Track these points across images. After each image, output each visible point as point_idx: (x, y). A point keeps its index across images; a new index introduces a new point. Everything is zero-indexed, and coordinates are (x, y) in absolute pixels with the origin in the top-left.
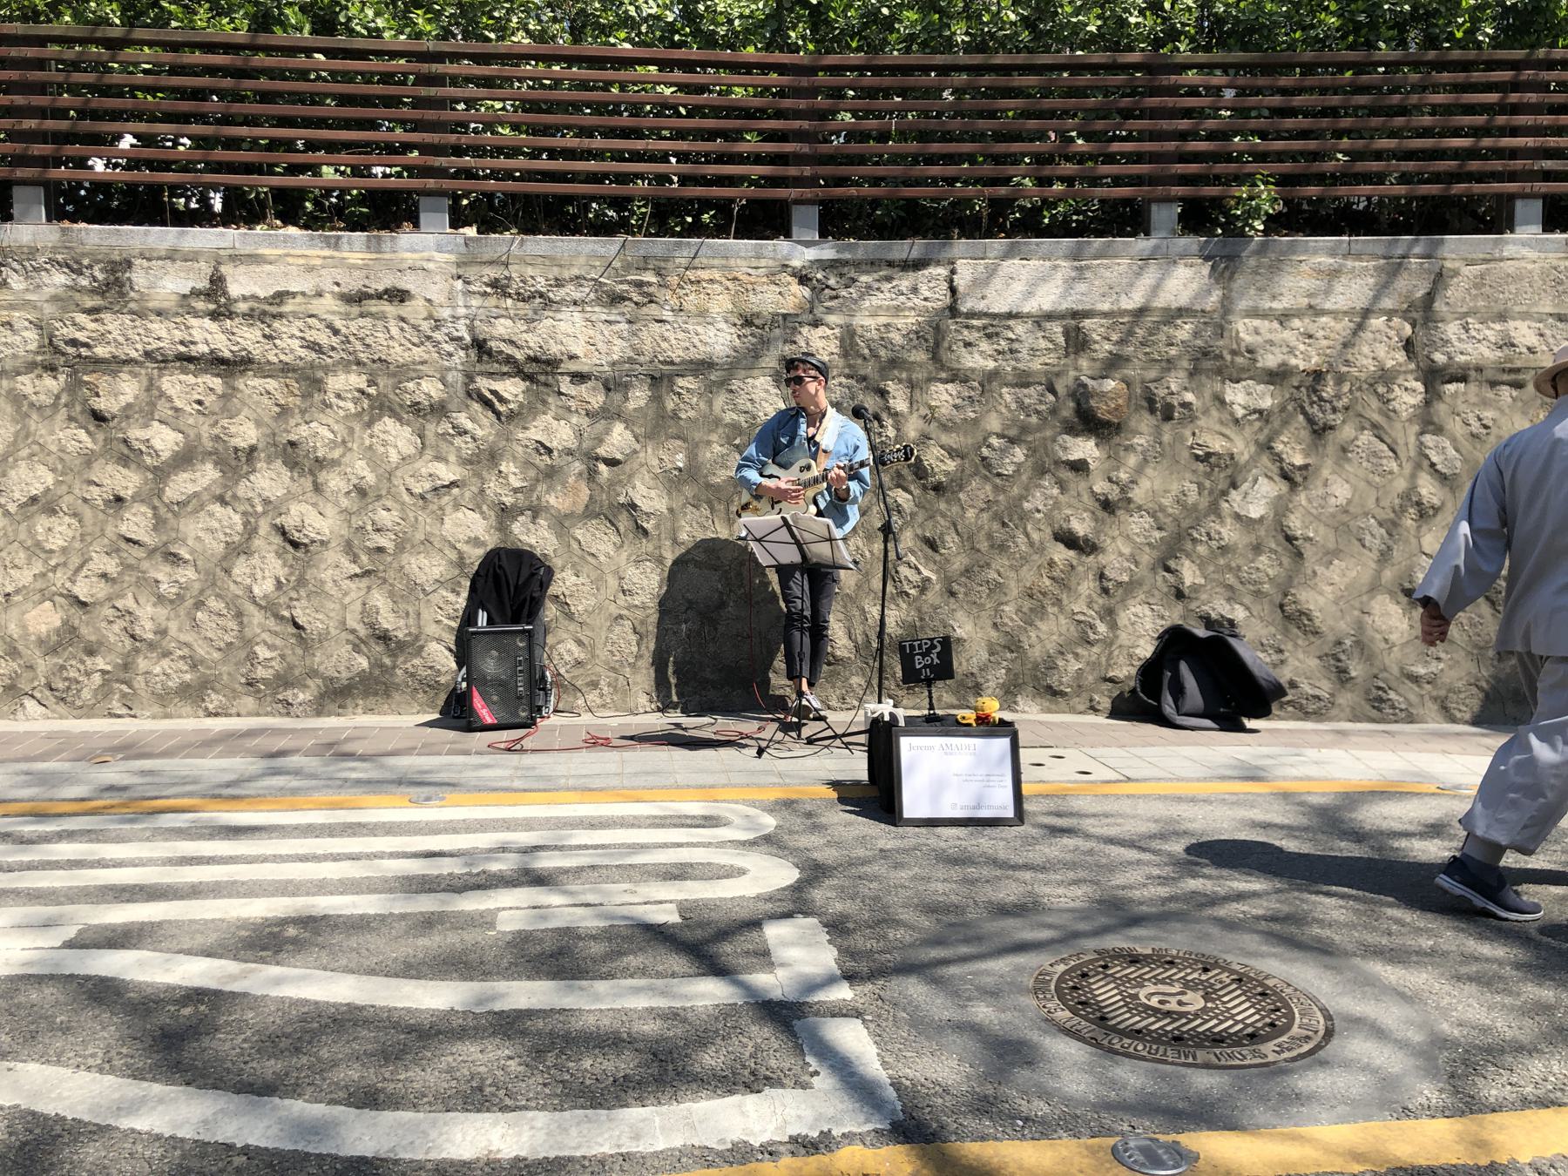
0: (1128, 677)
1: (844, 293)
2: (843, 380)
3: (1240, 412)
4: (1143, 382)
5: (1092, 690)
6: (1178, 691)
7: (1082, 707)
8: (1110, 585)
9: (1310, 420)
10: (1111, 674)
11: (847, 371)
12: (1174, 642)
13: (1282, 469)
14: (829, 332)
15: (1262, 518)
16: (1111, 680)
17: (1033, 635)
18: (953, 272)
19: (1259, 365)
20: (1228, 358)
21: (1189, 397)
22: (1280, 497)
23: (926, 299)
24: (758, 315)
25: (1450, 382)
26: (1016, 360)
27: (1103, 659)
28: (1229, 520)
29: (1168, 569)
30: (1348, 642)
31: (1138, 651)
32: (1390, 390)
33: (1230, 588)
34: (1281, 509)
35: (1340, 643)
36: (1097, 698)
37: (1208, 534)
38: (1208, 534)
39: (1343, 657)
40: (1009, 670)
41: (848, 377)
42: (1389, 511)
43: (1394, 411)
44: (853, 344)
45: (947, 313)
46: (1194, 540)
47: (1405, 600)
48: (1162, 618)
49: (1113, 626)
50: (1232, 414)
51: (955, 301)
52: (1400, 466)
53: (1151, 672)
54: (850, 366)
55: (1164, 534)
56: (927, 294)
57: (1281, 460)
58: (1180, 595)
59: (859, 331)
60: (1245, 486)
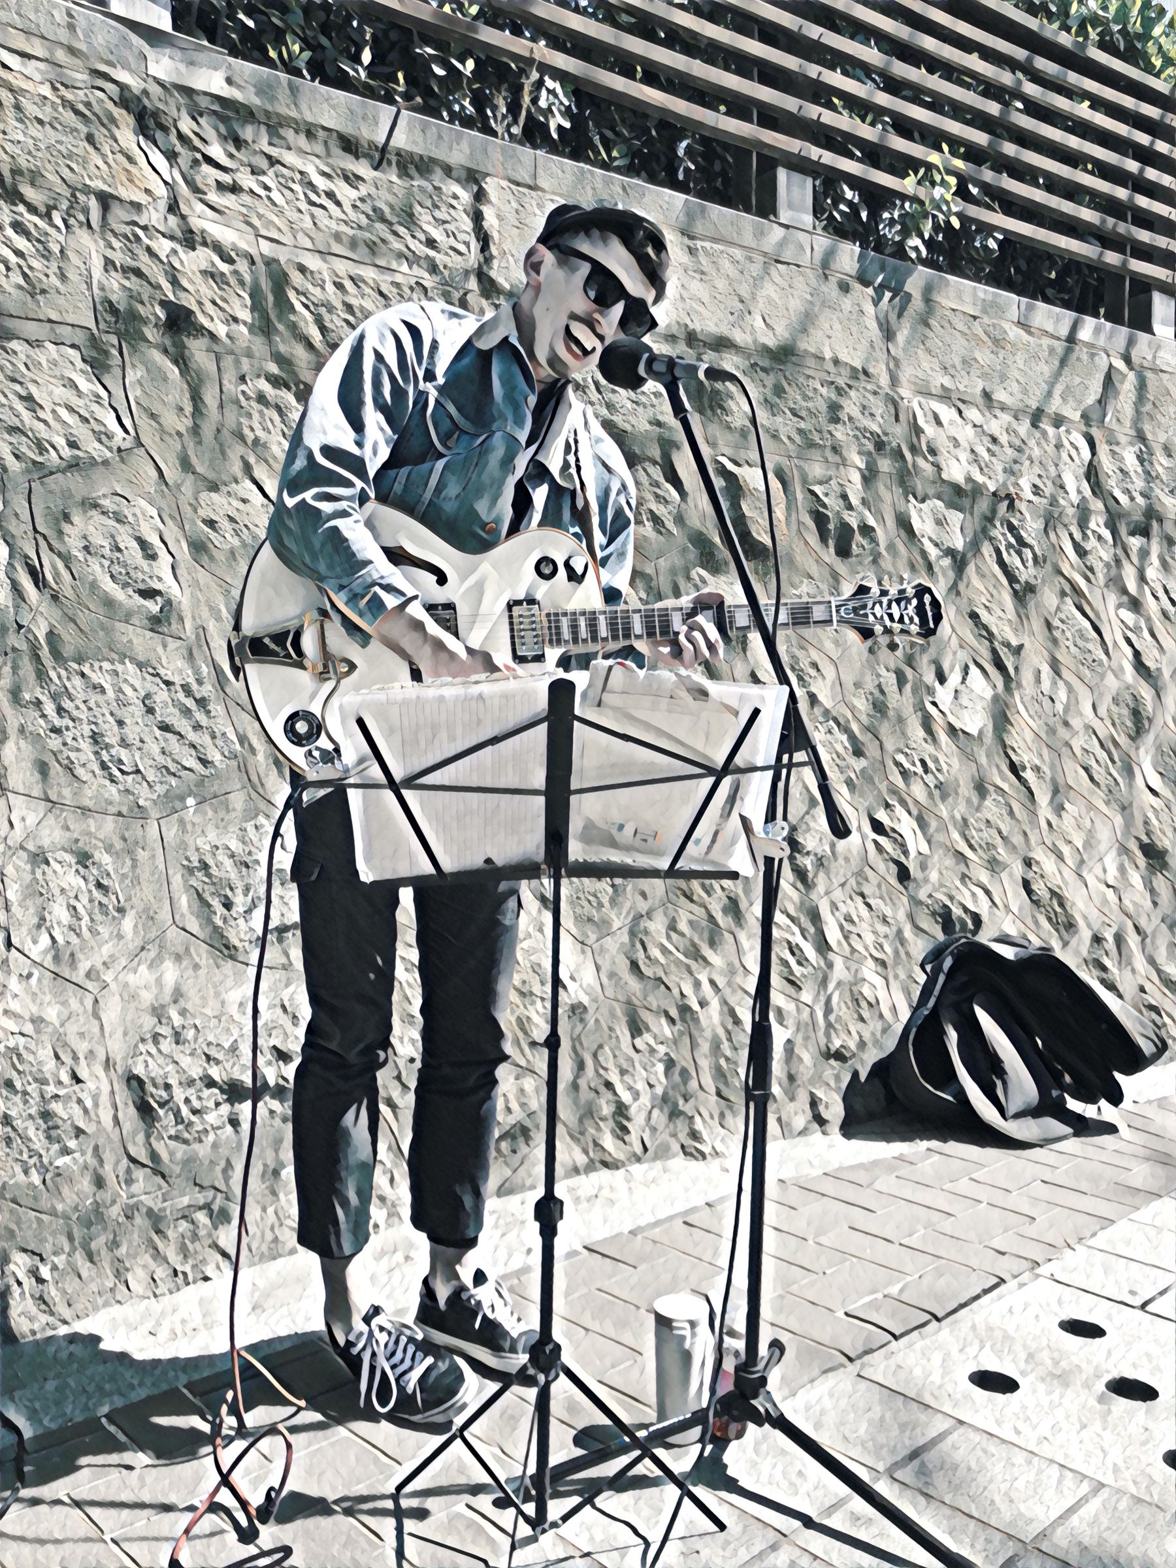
0: (862, 1044)
1: (247, 180)
2: (264, 386)
3: (933, 552)
4: (804, 481)
5: (812, 1081)
6: (988, 1070)
7: (800, 1120)
8: (808, 863)
9: (1011, 578)
10: (837, 1043)
11: (273, 368)
12: (966, 973)
13: (994, 651)
14: (224, 267)
15: (981, 732)
16: (839, 1056)
17: (703, 978)
18: (480, 196)
19: (944, 476)
20: (908, 456)
21: (871, 522)
22: (996, 699)
23: (431, 243)
24: (35, 177)
25: (1132, 533)
26: (610, 406)
27: (820, 1014)
28: (943, 737)
29: (878, 827)
30: (1109, 936)
31: (866, 991)
32: (1085, 536)
33: (960, 855)
34: (1001, 718)
35: (1097, 940)
36: (820, 1093)
37: (923, 762)
38: (923, 762)
39: (1107, 962)
40: (670, 1064)
41: (275, 381)
42: (1108, 723)
43: (1091, 569)
44: (283, 305)
45: (473, 284)
46: (905, 774)
47: (1141, 861)
48: (885, 921)
49: (823, 946)
50: (924, 554)
51: (488, 260)
52: (1107, 653)
53: (924, 1033)
54: (280, 359)
55: (863, 763)
56: (437, 234)
57: (990, 637)
58: (904, 875)
59: (296, 278)
60: (954, 679)
